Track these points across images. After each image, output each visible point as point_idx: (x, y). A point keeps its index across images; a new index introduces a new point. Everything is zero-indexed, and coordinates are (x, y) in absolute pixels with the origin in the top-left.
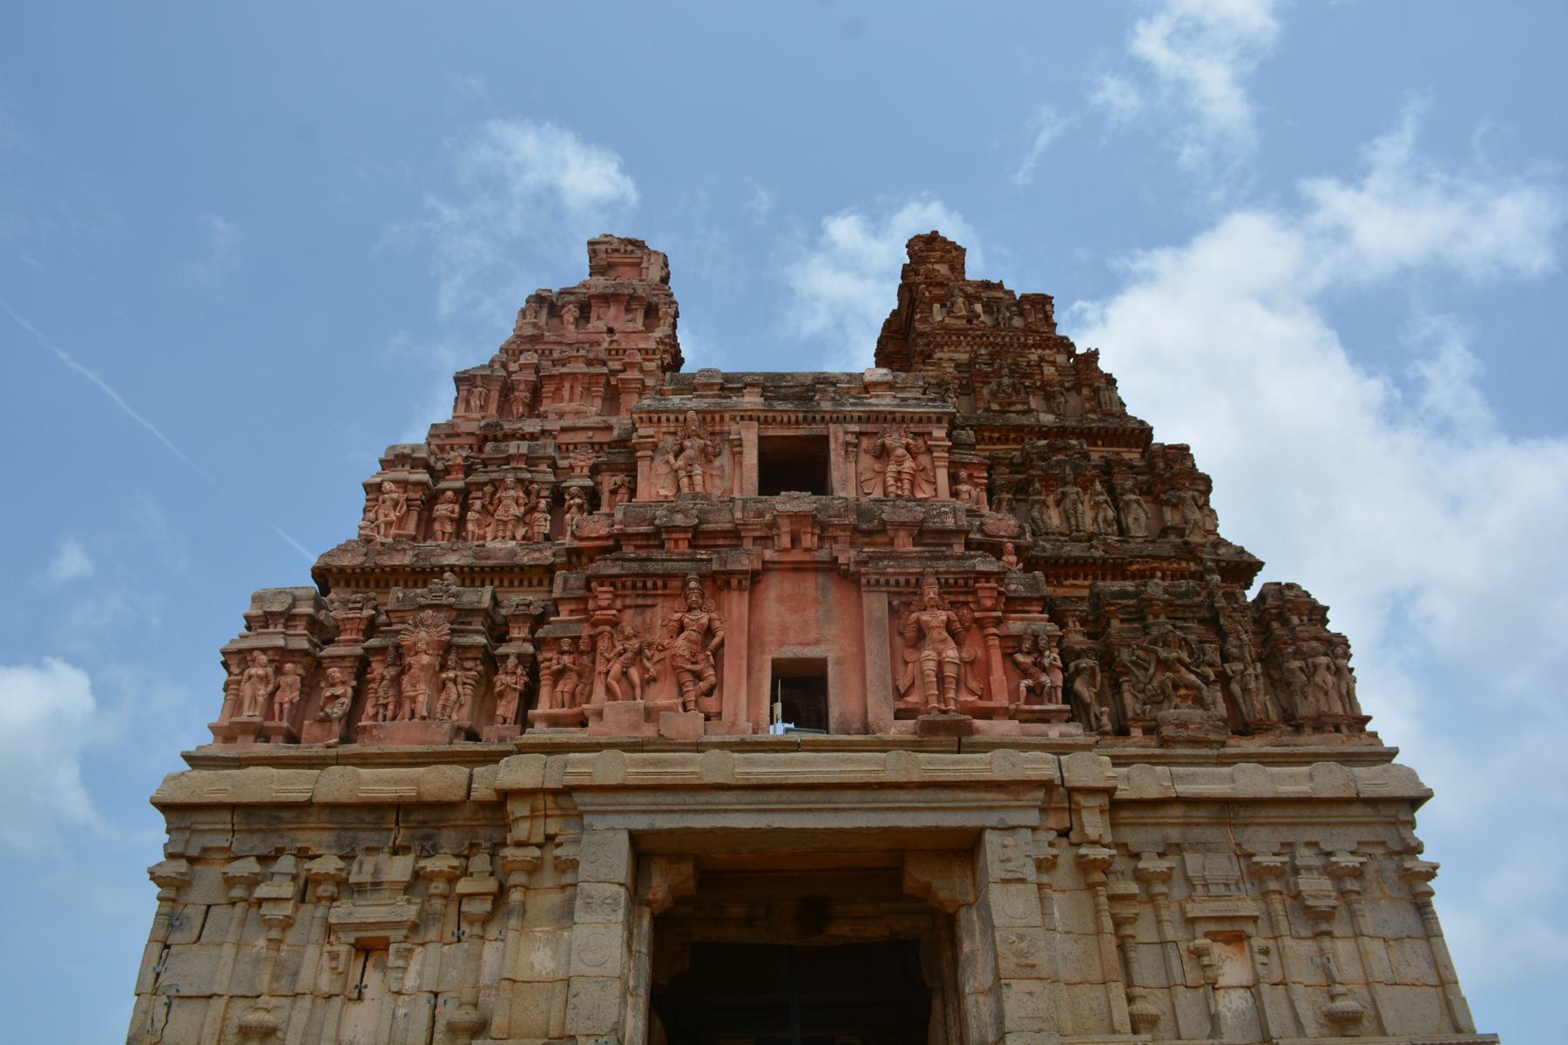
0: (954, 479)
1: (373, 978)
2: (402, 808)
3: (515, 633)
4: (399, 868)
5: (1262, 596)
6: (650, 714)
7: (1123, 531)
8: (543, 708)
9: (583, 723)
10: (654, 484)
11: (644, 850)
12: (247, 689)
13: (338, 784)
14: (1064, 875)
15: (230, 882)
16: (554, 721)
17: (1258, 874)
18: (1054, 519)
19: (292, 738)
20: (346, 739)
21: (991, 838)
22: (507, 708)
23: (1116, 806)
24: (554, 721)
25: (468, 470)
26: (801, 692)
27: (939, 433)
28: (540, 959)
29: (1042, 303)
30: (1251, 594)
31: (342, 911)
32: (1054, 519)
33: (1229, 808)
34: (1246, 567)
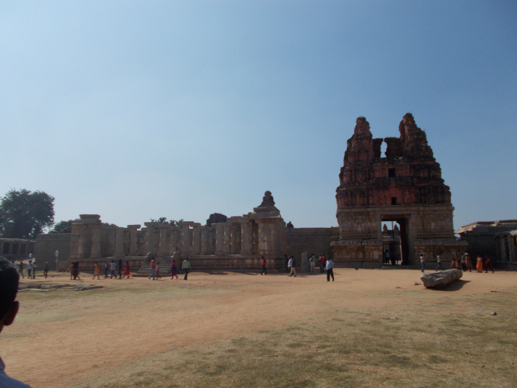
0: (410, 172)
1: (359, 226)
2: (359, 212)
3: (366, 193)
4: (360, 217)
6: (381, 204)
7: (429, 176)
8: (370, 202)
9: (374, 204)
11: (381, 215)
16: (372, 204)
19: (347, 205)
20: (352, 205)
21: (412, 215)
22: (366, 201)
24: (372, 204)
25: (355, 171)
27: (409, 167)
28: (374, 224)
32: (422, 175)
33: (435, 211)
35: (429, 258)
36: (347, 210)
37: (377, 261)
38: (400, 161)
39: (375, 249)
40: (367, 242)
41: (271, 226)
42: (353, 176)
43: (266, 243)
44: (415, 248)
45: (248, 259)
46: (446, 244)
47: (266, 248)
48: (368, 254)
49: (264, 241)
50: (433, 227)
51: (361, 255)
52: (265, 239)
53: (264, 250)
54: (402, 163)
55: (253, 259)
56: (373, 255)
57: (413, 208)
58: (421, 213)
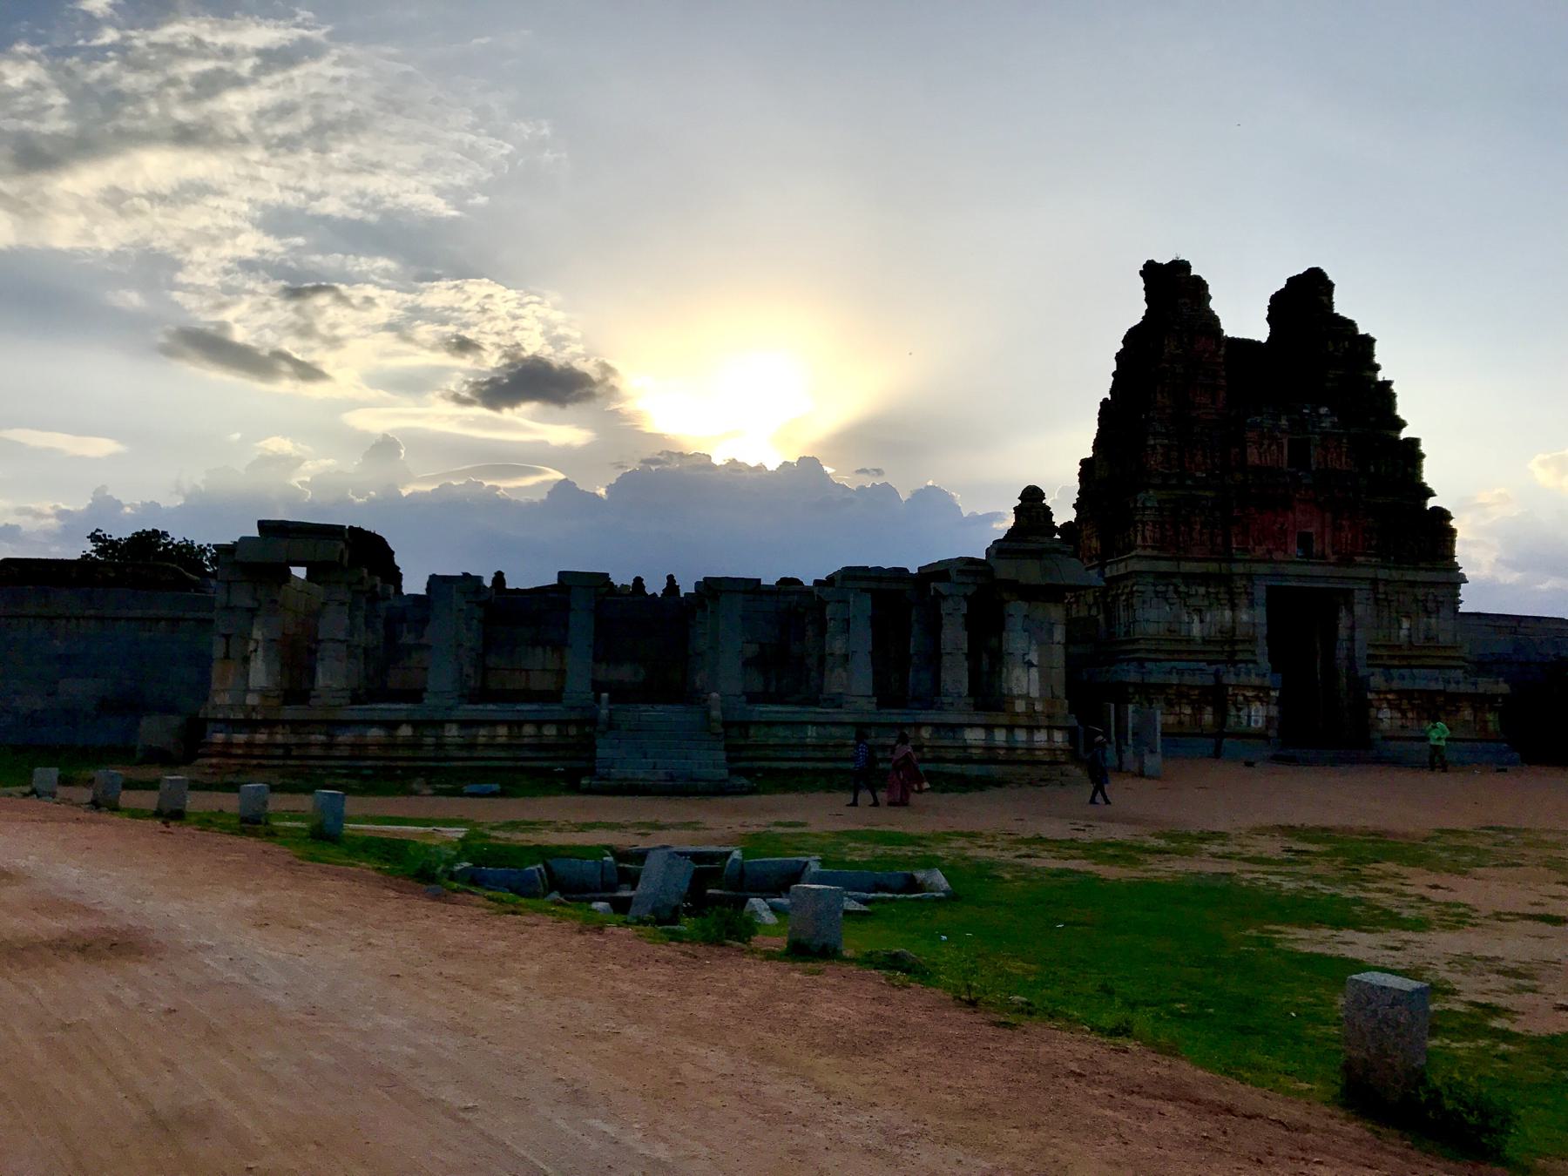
4: (1202, 590)
5: (1435, 509)
10: (1253, 457)
12: (1148, 534)
13: (1187, 567)
14: (1371, 602)
15: (1156, 592)
17: (1416, 600)
18: (1372, 469)
22: (1219, 540)
23: (1387, 582)
26: (1305, 541)
28: (1245, 617)
29: (1368, 342)
30: (1431, 503)
31: (1190, 601)
33: (1413, 584)
34: (1431, 493)
35: (1403, 727)
36: (1164, 566)
37: (1260, 735)
38: (1320, 416)
39: (1257, 698)
40: (1237, 675)
41: (1056, 613)
42: (1175, 454)
43: (1034, 672)
44: (1370, 696)
45: (971, 726)
46: (1452, 688)
47: (1035, 693)
48: (1233, 712)
49: (1030, 664)
50: (1404, 633)
51: (1208, 717)
52: (1034, 657)
53: (1026, 697)
54: (1326, 424)
55: (989, 728)
56: (1249, 717)
57: (1363, 573)
58: (1381, 589)
